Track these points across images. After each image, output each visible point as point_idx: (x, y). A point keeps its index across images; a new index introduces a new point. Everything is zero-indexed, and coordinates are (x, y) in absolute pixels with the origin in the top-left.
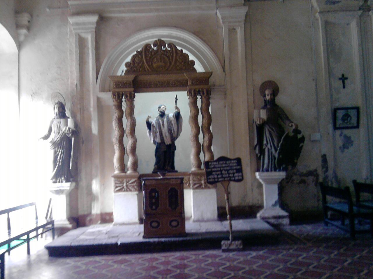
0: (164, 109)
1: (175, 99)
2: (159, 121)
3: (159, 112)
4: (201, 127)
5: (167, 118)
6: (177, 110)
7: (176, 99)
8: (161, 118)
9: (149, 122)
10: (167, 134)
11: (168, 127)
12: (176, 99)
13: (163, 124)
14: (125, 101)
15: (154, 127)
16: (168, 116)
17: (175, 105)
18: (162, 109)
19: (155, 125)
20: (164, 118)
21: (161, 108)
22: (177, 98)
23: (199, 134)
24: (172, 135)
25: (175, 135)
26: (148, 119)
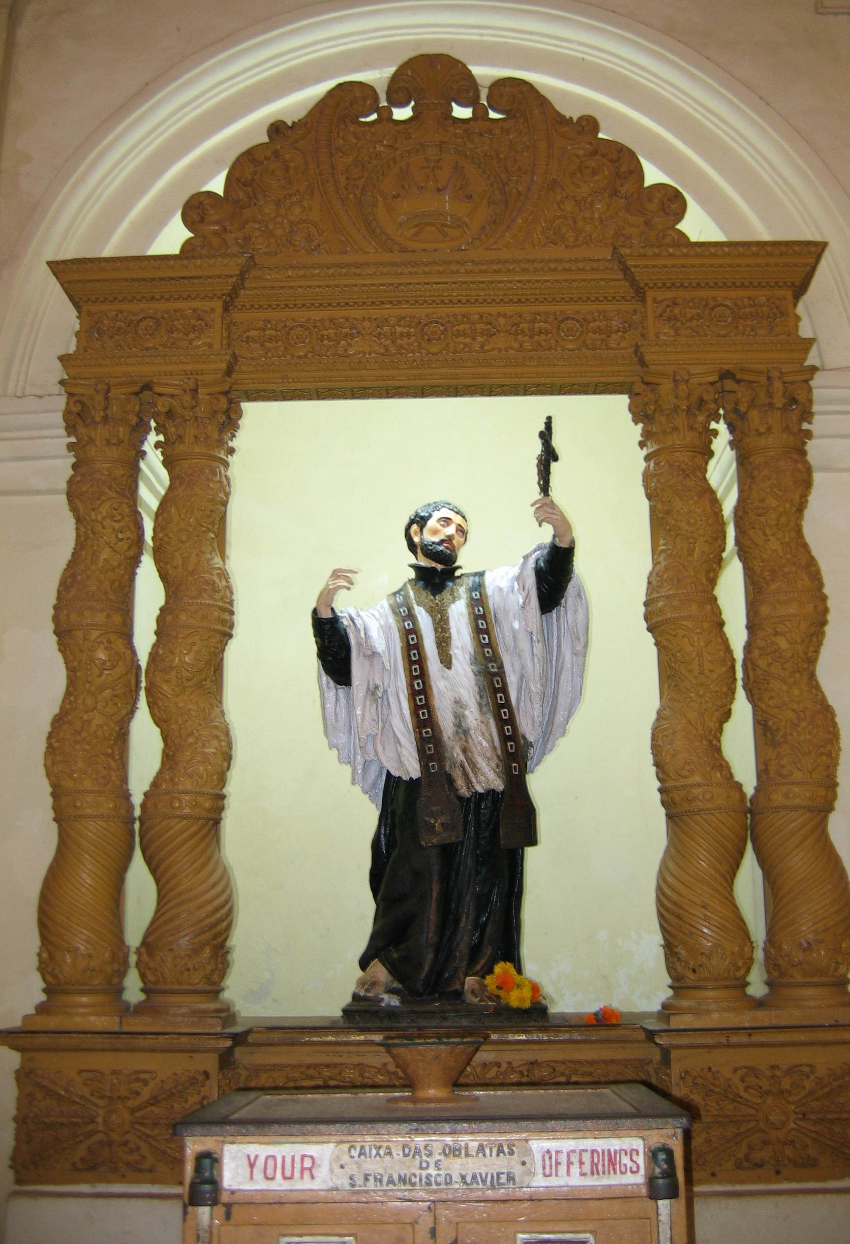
0: (451, 530)
1: (537, 447)
2: (411, 616)
3: (412, 560)
4: (739, 655)
5: (476, 595)
6: (545, 535)
7: (549, 456)
8: (426, 596)
9: (335, 620)
10: (473, 716)
11: (474, 661)
12: (549, 456)
13: (443, 642)
14: (158, 445)
15: (373, 655)
16: (479, 587)
17: (535, 493)
18: (435, 532)
19: (380, 645)
20: (446, 594)
21: (431, 523)
22: (557, 442)
23: (727, 715)
24: (511, 721)
25: (528, 727)
26: (327, 595)
